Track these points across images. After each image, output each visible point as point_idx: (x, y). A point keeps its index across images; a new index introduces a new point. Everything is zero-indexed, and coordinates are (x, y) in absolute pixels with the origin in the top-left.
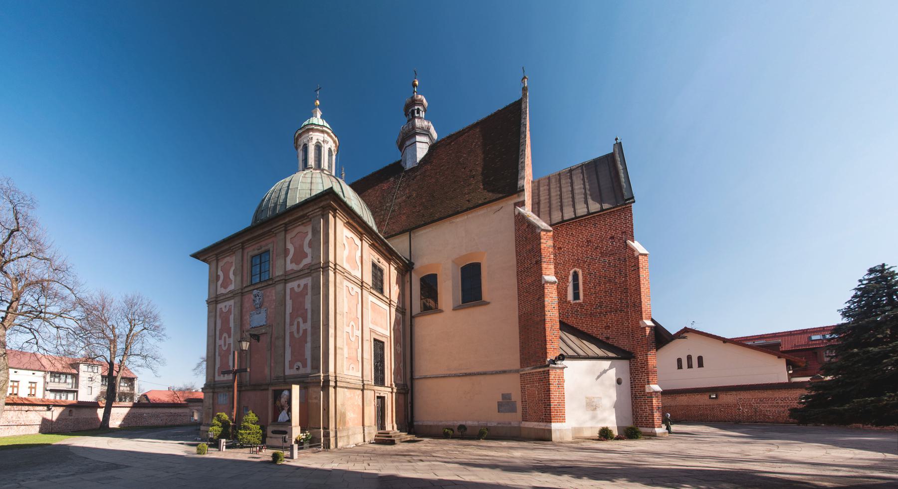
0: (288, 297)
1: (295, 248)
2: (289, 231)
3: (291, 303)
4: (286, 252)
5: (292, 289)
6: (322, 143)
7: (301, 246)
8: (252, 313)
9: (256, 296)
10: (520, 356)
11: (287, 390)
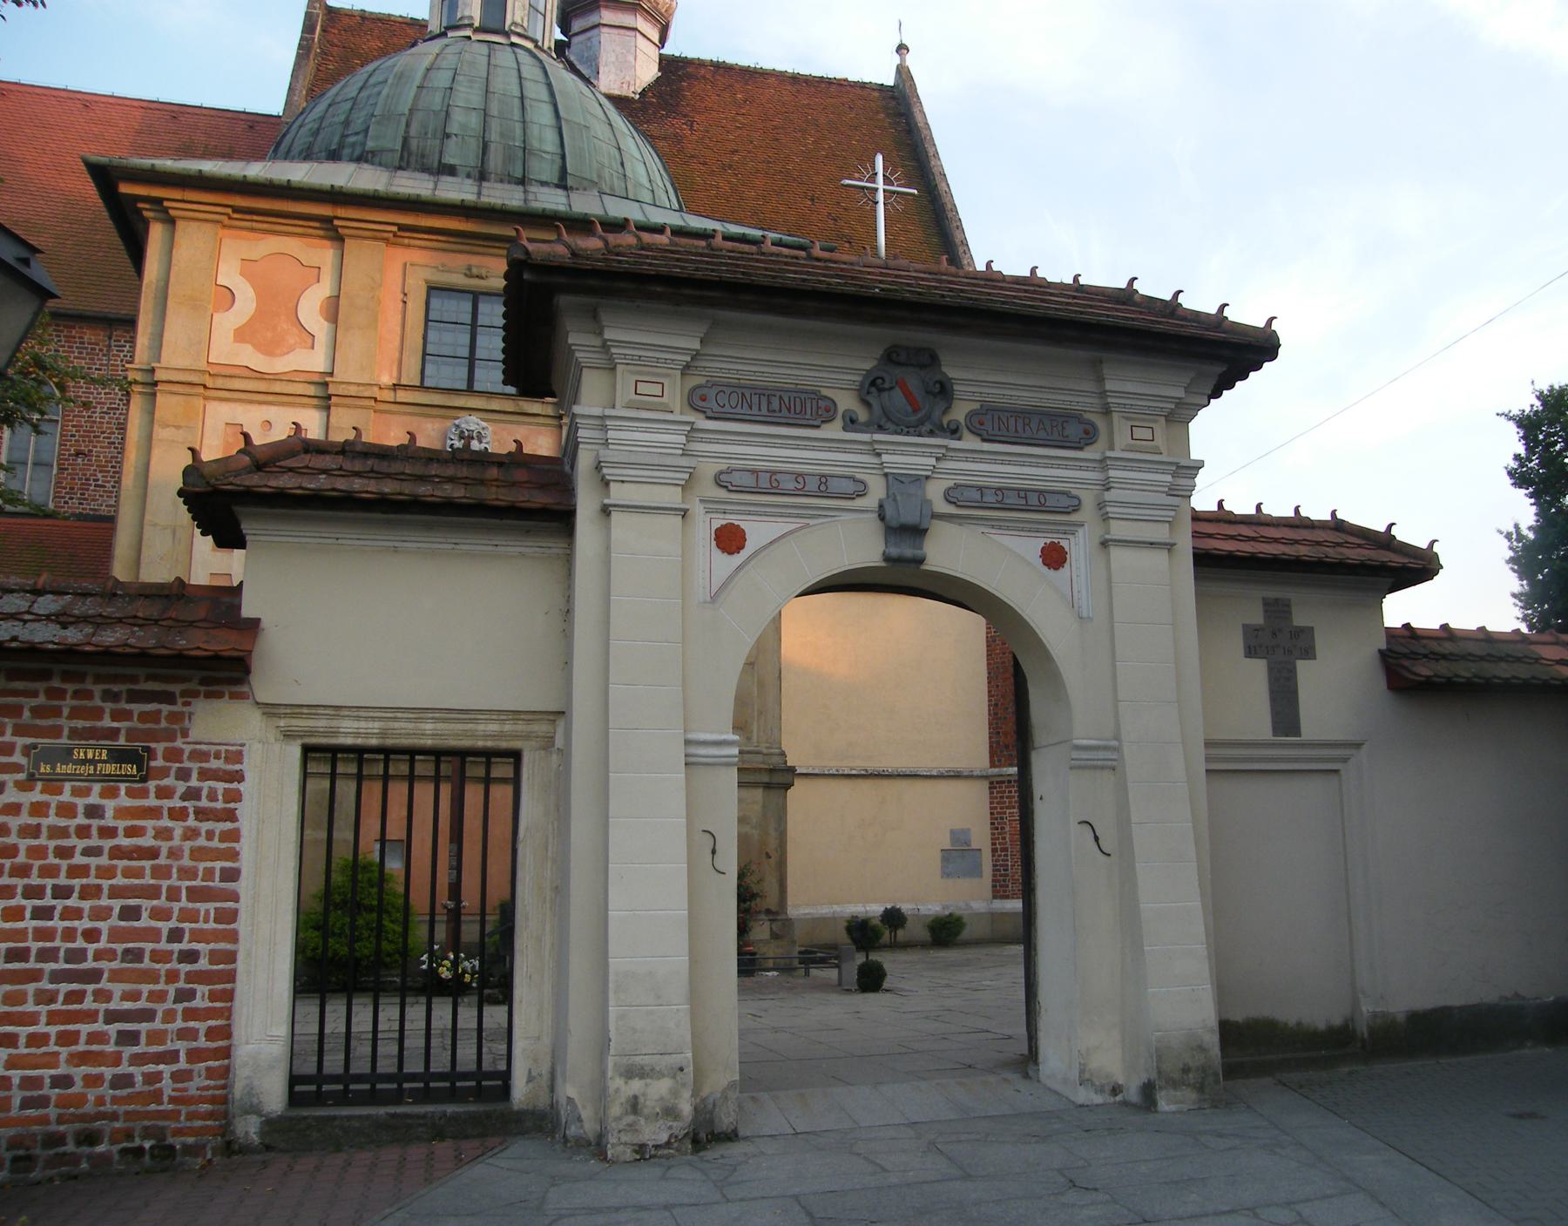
10: (990, 738)
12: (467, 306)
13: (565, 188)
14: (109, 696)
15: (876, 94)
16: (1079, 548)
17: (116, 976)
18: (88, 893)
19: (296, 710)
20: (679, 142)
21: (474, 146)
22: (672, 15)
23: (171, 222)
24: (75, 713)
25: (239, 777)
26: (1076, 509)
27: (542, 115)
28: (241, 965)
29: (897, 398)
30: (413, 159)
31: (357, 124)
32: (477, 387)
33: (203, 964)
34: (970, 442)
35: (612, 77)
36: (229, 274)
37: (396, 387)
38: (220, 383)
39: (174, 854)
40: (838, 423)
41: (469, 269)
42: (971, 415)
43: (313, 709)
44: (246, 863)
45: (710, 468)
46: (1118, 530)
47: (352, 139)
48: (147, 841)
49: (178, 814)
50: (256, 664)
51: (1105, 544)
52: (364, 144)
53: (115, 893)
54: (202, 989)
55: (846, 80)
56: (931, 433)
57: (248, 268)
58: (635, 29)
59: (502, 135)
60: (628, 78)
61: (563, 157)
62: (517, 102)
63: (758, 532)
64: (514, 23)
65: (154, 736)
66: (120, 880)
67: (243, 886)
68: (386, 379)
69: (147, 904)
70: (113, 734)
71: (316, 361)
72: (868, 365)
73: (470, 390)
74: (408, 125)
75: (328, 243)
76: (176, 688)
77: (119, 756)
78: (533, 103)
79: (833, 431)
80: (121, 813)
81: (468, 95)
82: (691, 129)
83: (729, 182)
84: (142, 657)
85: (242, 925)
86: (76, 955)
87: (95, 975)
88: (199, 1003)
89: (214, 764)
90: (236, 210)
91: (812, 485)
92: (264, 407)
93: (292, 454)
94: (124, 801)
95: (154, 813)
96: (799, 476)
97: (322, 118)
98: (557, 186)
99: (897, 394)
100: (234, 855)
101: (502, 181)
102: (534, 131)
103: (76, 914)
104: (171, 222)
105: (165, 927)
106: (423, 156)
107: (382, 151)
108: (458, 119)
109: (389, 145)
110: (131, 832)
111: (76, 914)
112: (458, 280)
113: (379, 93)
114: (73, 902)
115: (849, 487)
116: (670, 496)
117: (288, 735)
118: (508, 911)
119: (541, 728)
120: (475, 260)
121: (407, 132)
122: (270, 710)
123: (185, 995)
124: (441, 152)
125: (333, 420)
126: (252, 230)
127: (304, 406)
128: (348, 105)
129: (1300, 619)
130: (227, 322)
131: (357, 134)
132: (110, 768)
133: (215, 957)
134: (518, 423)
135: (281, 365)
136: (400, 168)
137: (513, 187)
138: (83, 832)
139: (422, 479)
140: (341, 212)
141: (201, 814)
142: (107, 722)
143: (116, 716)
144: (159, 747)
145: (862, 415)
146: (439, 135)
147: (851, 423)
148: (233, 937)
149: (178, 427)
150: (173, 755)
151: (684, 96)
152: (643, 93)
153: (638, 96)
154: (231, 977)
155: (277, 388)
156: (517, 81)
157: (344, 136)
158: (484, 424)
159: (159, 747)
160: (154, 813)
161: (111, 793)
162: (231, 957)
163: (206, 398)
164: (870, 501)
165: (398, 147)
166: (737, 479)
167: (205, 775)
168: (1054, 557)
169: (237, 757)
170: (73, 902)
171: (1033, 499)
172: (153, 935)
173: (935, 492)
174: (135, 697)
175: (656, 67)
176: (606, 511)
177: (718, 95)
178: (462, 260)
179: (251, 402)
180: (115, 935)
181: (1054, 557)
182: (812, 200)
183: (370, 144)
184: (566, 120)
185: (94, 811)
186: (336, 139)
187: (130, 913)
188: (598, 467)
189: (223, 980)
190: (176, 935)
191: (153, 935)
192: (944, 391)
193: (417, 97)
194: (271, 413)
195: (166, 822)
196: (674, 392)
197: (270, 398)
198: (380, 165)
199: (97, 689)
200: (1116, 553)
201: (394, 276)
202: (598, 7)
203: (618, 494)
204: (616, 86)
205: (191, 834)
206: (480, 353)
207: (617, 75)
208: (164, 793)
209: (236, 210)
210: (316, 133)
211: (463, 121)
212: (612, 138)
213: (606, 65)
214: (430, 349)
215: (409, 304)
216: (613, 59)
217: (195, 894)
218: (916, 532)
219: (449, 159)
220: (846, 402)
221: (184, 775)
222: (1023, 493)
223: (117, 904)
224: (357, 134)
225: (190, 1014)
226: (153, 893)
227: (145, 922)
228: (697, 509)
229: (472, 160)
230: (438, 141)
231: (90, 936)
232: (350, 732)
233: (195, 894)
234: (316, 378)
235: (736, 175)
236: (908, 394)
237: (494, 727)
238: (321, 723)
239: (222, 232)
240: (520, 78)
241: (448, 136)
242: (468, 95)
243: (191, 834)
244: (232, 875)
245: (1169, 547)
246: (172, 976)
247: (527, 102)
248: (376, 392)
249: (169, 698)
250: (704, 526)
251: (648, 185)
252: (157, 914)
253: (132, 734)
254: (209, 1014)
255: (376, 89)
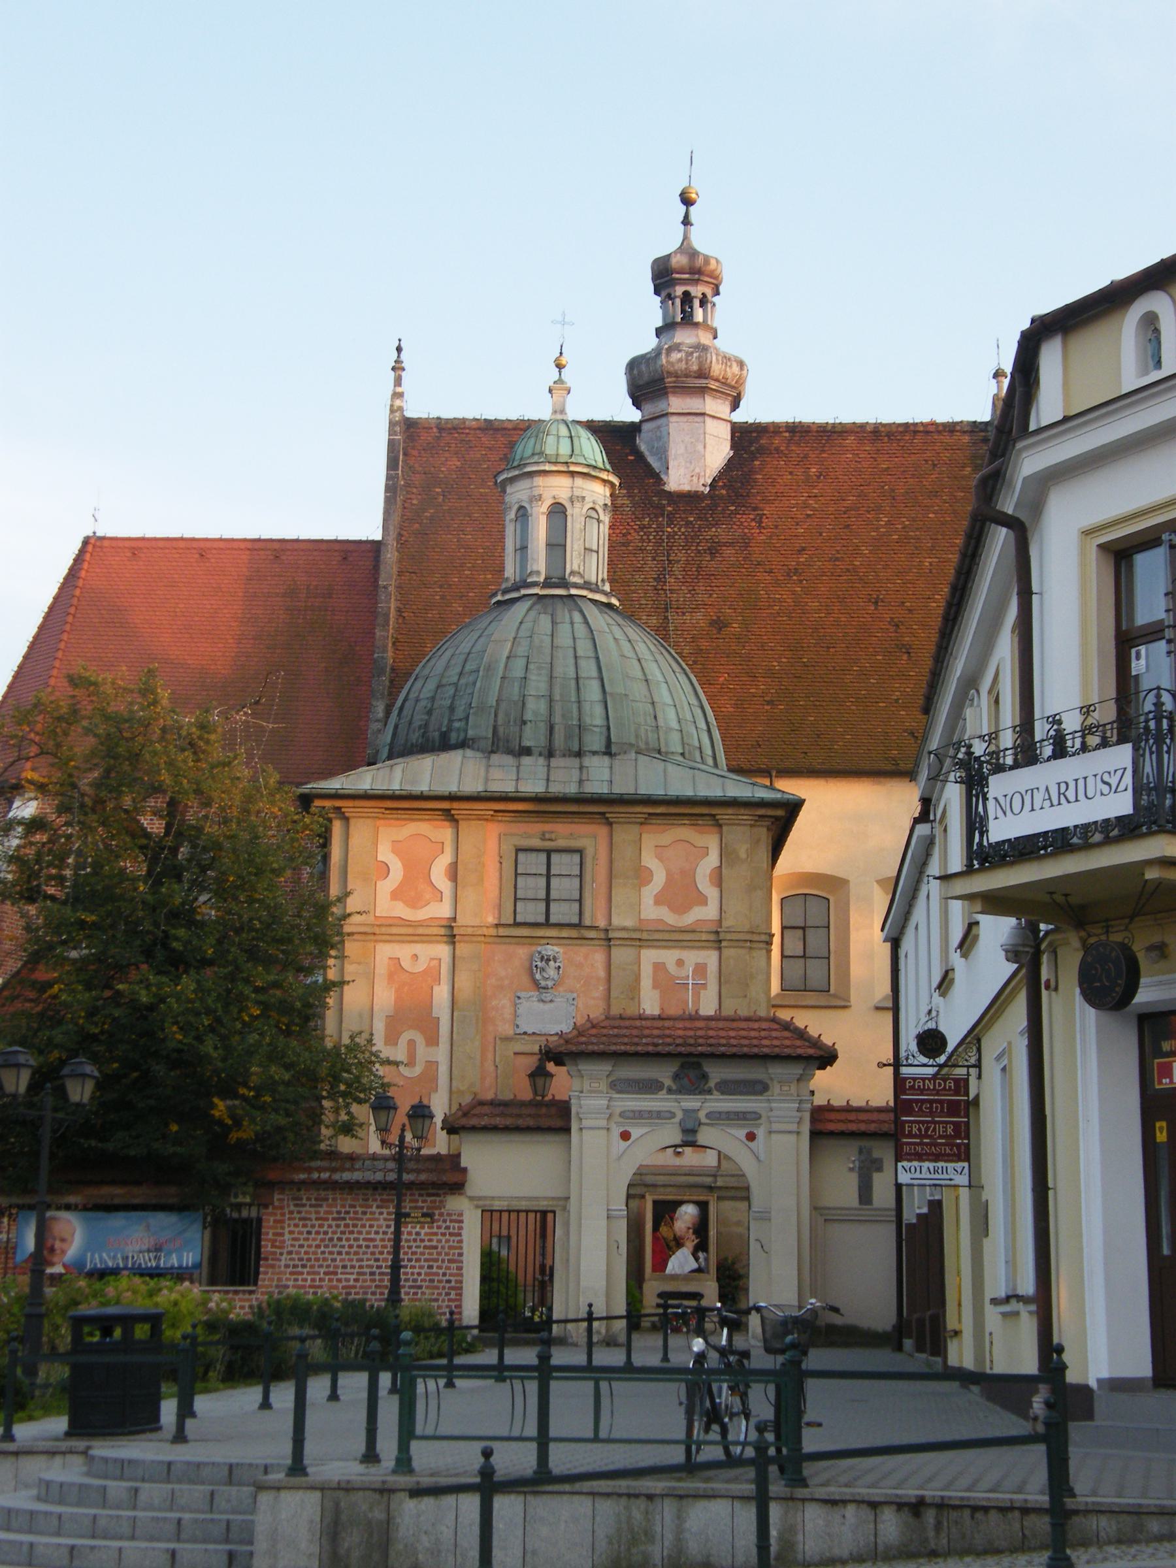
0: (646, 982)
1: (669, 875)
2: (649, 827)
3: (657, 996)
4: (642, 876)
5: (659, 967)
6: (567, 505)
7: (689, 875)
8: (522, 994)
9: (548, 960)
11: (697, 1203)
12: (543, 857)
13: (608, 752)
14: (421, 1195)
15: (966, 439)
16: (760, 1133)
17: (427, 1287)
18: (418, 1260)
19: (480, 1198)
20: (747, 545)
21: (543, 728)
22: (743, 383)
23: (346, 820)
24: (411, 1201)
25: (462, 1222)
26: (760, 1117)
27: (592, 692)
28: (464, 1285)
29: (685, 1081)
30: (501, 744)
31: (460, 712)
32: (553, 920)
33: (453, 1284)
34: (716, 1095)
35: (682, 471)
36: (385, 854)
37: (497, 926)
38: (383, 930)
39: (443, 1247)
40: (664, 1091)
41: (543, 835)
42: (716, 1084)
43: (485, 1198)
44: (465, 1251)
45: (618, 1111)
46: (775, 1127)
47: (457, 725)
48: (434, 1243)
49: (443, 1234)
50: (467, 1185)
51: (770, 1132)
52: (466, 731)
53: (426, 1260)
54: (453, 1292)
55: (933, 424)
56: (700, 1093)
57: (397, 848)
58: (703, 414)
59: (563, 716)
60: (697, 470)
61: (608, 728)
62: (573, 683)
63: (635, 1132)
64: (572, 573)
65: (436, 1208)
66: (426, 1256)
67: (464, 1258)
68: (491, 920)
69: (435, 1264)
70: (422, 1208)
71: (444, 910)
72: (674, 1070)
73: (547, 924)
74: (496, 716)
75: (447, 824)
76: (441, 1192)
77: (424, 1215)
78: (587, 682)
79: (663, 1094)
80: (426, 1234)
81: (538, 684)
82: (760, 527)
83: (794, 593)
84: (434, 1185)
85: (464, 1271)
86: (415, 1280)
87: (420, 1287)
88: (452, 1296)
89: (454, 1217)
90: (387, 809)
91: (655, 1115)
92: (413, 945)
93: (474, 1107)
94: (426, 1230)
95: (436, 1234)
96: (650, 1112)
97: (433, 699)
98: (605, 754)
99: (686, 1080)
100: (461, 1248)
101: (564, 756)
102: (586, 707)
103: (413, 1267)
104: (346, 820)
105: (441, 1272)
106: (508, 741)
107: (480, 738)
108: (531, 704)
109: (484, 734)
110: (430, 1240)
111: (414, 1267)
112: (536, 842)
113: (474, 683)
114: (413, 1263)
115: (668, 1115)
116: (603, 1123)
117: (477, 1207)
118: (552, 1269)
119: (561, 1203)
120: (547, 827)
121: (495, 721)
122: (471, 1198)
123: (448, 1294)
124: (520, 737)
125: (458, 952)
126: (398, 819)
127: (438, 942)
128: (451, 691)
129: (876, 1154)
130: (386, 887)
131: (460, 720)
132: (422, 1220)
133: (457, 1282)
134: (581, 945)
135: (422, 914)
136: (493, 752)
137: (573, 759)
138: (415, 1240)
139: (519, 1116)
140: (456, 805)
141: (451, 1234)
142: (420, 1204)
143: (423, 1202)
144: (437, 1212)
145: (674, 1088)
146: (519, 723)
147: (670, 1091)
148: (461, 1275)
149: (359, 963)
150: (441, 1214)
151: (755, 481)
152: (713, 485)
153: (708, 489)
154: (461, 1288)
155: (421, 931)
156: (572, 661)
157: (451, 721)
158: (556, 949)
159: (437, 1212)
160: (436, 1234)
161: (422, 1228)
162: (461, 1282)
163: (376, 941)
164: (677, 1120)
165: (490, 735)
166: (628, 1114)
167: (451, 1221)
168: (751, 1137)
169: (461, 1215)
170: (413, 1263)
171: (741, 1116)
172: (437, 1274)
173: (702, 1115)
174: (429, 1195)
175: (728, 445)
176: (581, 1129)
177: (791, 473)
178: (538, 828)
179: (403, 942)
180: (426, 1274)
181: (751, 1137)
182: (876, 603)
183: (471, 733)
184: (611, 694)
185: (418, 1234)
186: (446, 722)
187: (430, 1267)
188: (578, 1114)
189: (459, 1289)
190: (444, 1274)
191: (437, 1274)
192: (705, 1077)
193: (501, 687)
194: (418, 948)
195: (439, 1237)
196: (603, 1086)
197: (416, 938)
198: (478, 750)
199: (417, 1193)
200: (774, 1136)
201: (492, 844)
202: (666, 394)
203: (585, 1123)
204: (686, 481)
205: (447, 1241)
206: (553, 895)
207: (687, 468)
208: (439, 1227)
209: (387, 809)
210: (430, 712)
211: (535, 708)
212: (648, 694)
213: (675, 459)
214: (520, 894)
215: (504, 865)
216: (681, 450)
217: (450, 1261)
218: (694, 1132)
219: (527, 743)
220: (668, 1082)
221: (445, 1221)
222: (737, 1113)
223: (426, 1264)
224: (460, 720)
225: (449, 1300)
226: (436, 1260)
227: (435, 1270)
228: (613, 1126)
229: (543, 741)
230: (518, 728)
231: (419, 1274)
232: (497, 1205)
233: (450, 1261)
234: (445, 923)
235: (801, 581)
236: (690, 1080)
237: (545, 1203)
238: (488, 1202)
239: (379, 822)
240: (576, 657)
241: (524, 723)
242: (538, 684)
243: (447, 1241)
244: (461, 1255)
245: (798, 1133)
246: (444, 1288)
247: (581, 682)
248: (485, 931)
249: (438, 1195)
250: (616, 1132)
251: (677, 727)
252: (439, 1267)
253: (428, 1208)
254: (455, 1300)
255: (471, 679)
